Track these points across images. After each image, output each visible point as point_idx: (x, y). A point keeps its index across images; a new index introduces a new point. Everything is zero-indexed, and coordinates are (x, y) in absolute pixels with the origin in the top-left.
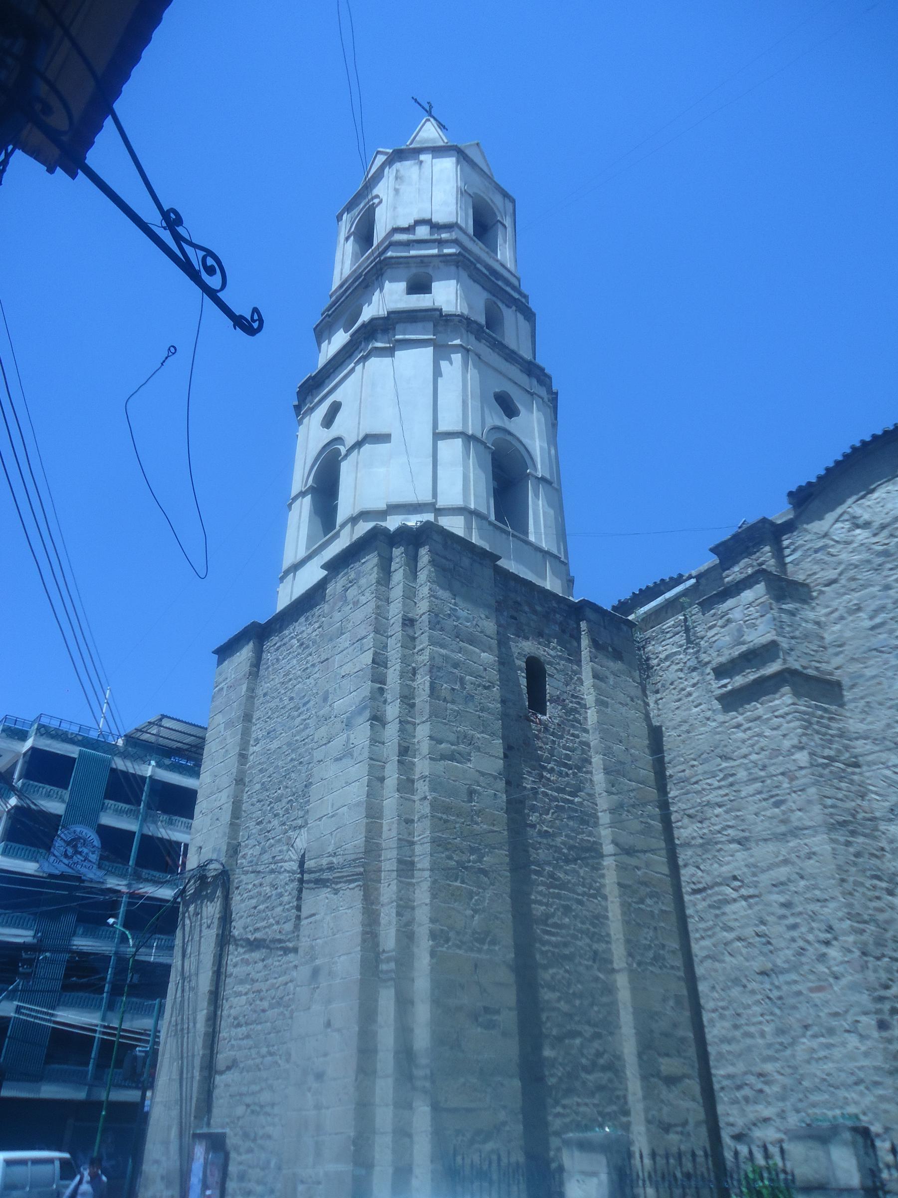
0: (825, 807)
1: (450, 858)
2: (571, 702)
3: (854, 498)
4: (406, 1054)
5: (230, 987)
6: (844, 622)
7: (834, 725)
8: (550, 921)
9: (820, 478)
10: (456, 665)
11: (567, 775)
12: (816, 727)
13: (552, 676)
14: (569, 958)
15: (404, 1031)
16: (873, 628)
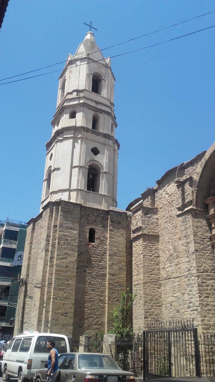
0: (144, 268)
1: (60, 282)
2: (103, 238)
3: (167, 185)
4: (47, 322)
5: (26, 306)
6: (162, 219)
7: (154, 247)
8: (88, 293)
9: (161, 179)
10: (66, 236)
11: (98, 257)
12: (148, 248)
13: (97, 232)
14: (93, 301)
15: (47, 317)
16: (165, 222)
